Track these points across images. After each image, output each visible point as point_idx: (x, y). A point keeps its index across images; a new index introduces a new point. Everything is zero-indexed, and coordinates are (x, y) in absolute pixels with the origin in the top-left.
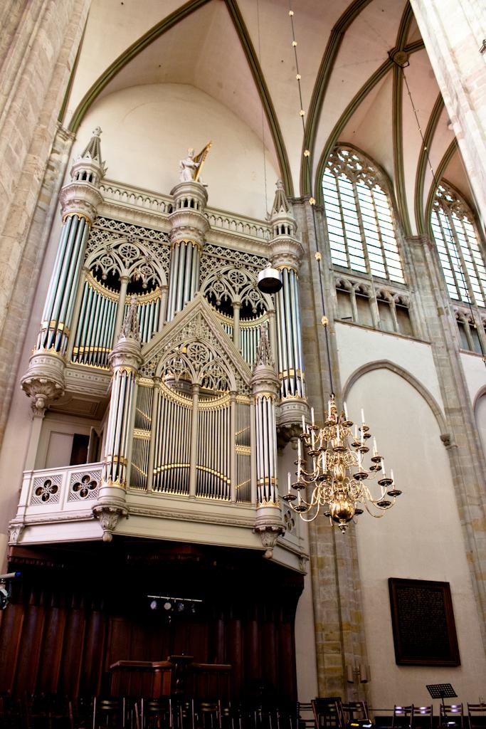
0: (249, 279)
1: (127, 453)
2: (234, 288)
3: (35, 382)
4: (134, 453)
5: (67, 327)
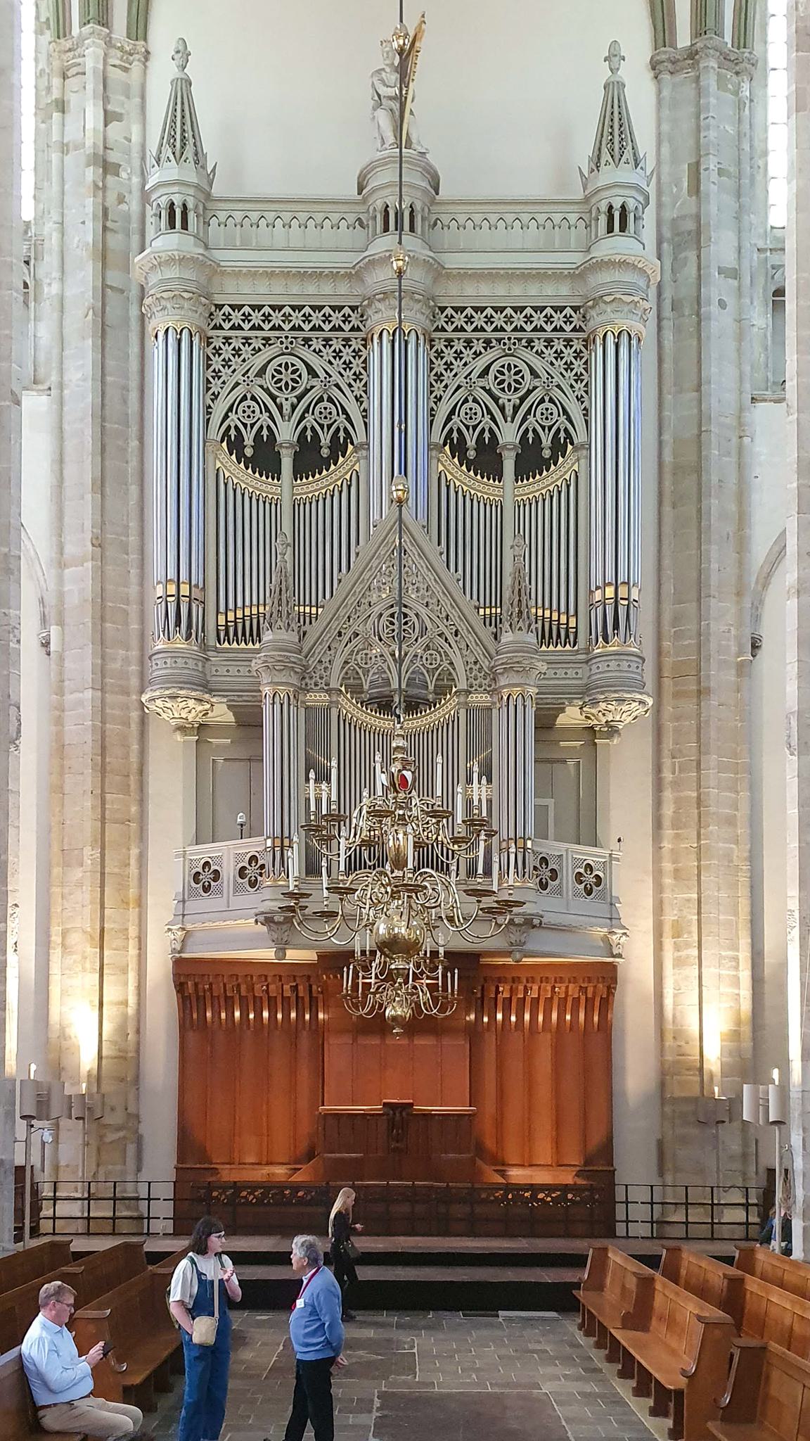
0: (534, 373)
5: (197, 586)
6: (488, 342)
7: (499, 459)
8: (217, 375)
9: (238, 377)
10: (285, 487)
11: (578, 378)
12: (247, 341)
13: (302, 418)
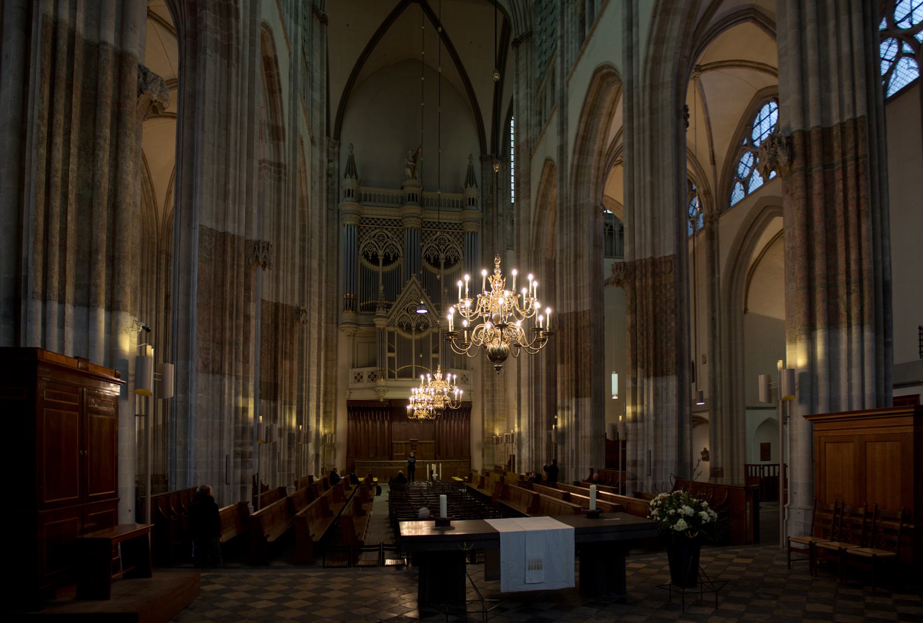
2: (441, 250)
7: (440, 265)
8: (362, 237)
9: (367, 238)
11: (461, 242)
13: (385, 249)
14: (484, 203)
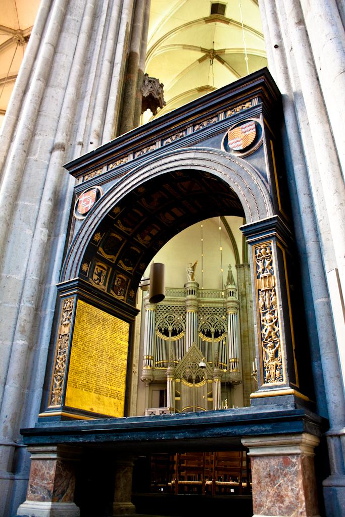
1: (173, 406)
3: (145, 380)
4: (176, 405)
6: (208, 314)
8: (157, 318)
10: (170, 339)
12: (163, 312)
14: (240, 294)
